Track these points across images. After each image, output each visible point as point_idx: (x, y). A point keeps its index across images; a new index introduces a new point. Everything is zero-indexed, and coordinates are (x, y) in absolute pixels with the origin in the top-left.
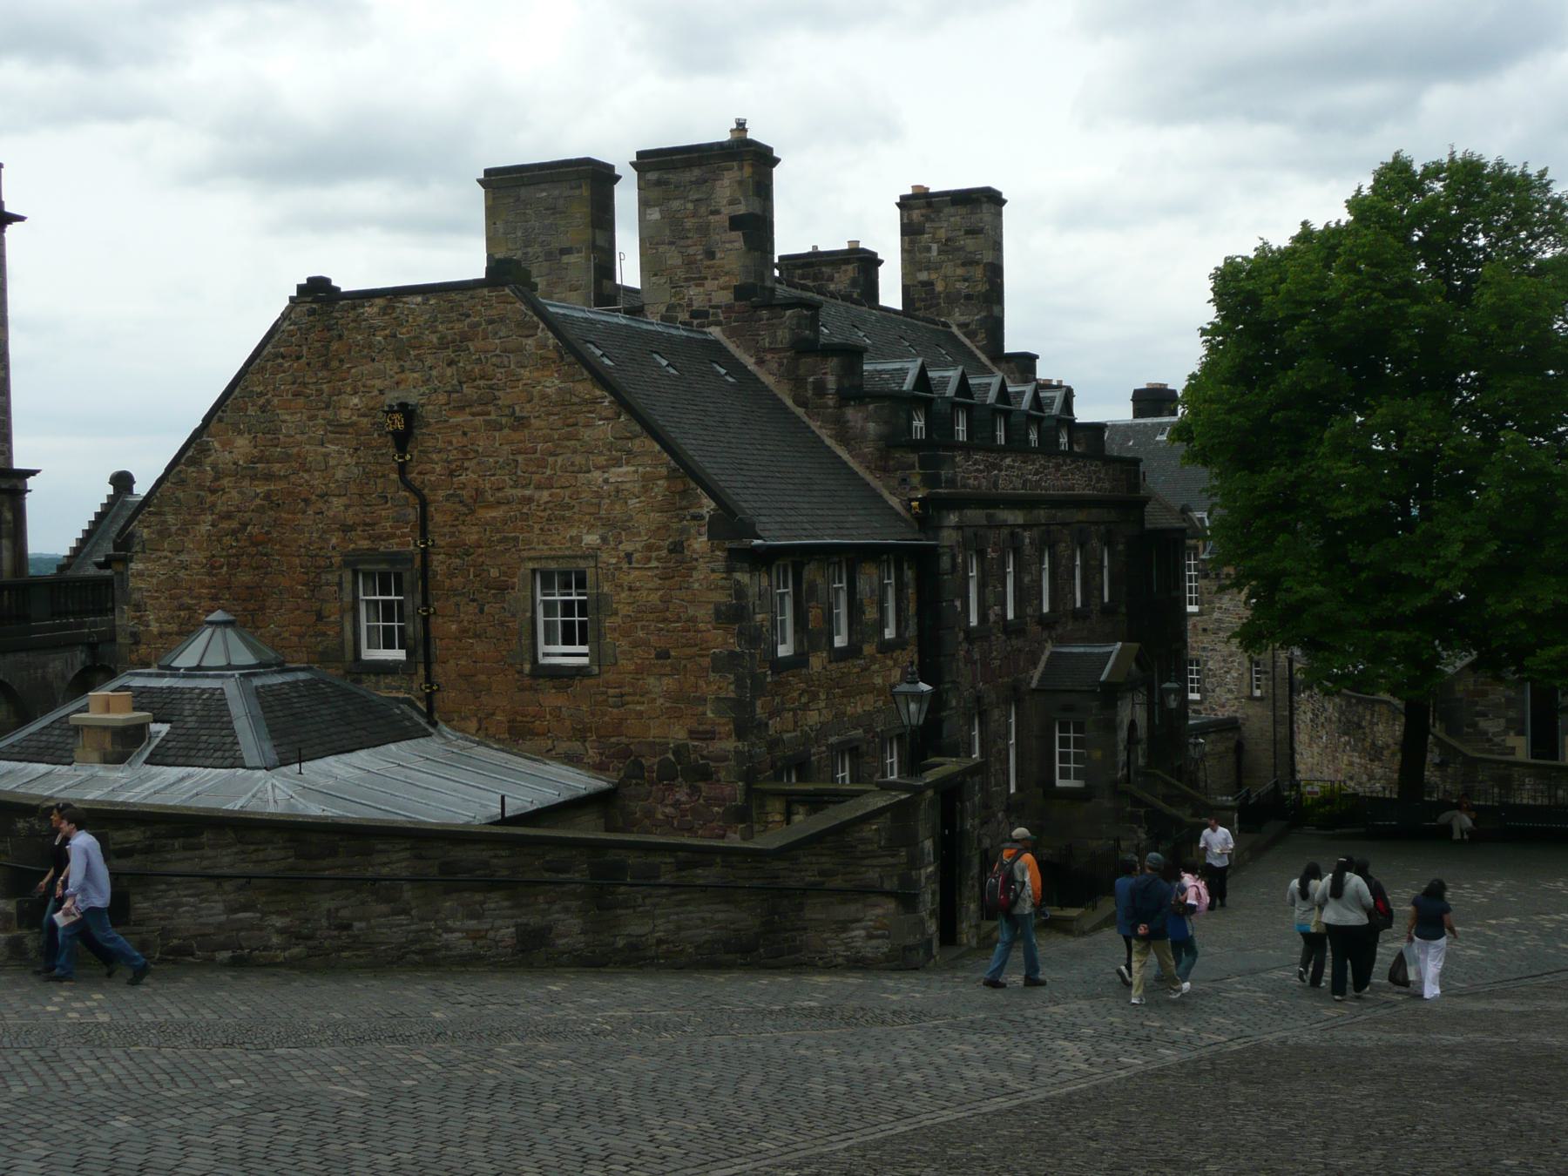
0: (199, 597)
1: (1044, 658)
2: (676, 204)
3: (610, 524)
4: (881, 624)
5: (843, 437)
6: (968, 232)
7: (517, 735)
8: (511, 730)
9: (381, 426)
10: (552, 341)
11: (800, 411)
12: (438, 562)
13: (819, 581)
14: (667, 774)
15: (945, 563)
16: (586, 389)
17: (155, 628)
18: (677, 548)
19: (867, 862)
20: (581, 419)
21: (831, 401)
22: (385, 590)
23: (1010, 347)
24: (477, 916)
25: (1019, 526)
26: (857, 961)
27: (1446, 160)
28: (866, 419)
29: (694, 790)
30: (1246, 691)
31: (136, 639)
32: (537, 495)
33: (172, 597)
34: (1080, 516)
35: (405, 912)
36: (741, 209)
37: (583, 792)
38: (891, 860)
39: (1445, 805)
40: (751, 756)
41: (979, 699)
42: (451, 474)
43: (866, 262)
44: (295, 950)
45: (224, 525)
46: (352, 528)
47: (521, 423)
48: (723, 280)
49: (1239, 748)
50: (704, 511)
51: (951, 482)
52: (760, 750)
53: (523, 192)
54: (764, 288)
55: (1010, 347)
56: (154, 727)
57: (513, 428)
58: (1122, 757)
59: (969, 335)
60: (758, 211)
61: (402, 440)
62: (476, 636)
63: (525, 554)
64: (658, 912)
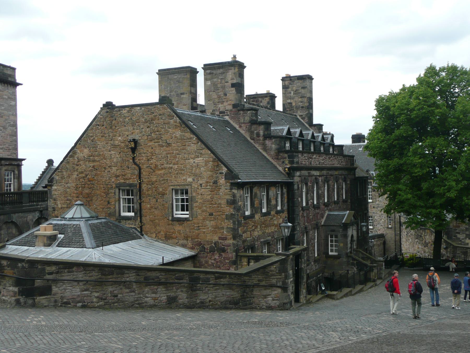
0: (73, 197)
1: (326, 216)
2: (215, 80)
3: (195, 175)
4: (276, 205)
5: (265, 149)
6: (302, 88)
7: (168, 238)
8: (166, 237)
9: (127, 146)
10: (178, 120)
11: (252, 141)
12: (144, 186)
13: (258, 192)
14: (212, 250)
15: (296, 187)
18: (215, 182)
19: (272, 277)
20: (187, 143)
21: (261, 138)
22: (128, 195)
23: (315, 122)
24: (156, 293)
25: (318, 176)
26: (269, 307)
27: (446, 66)
28: (272, 144)
29: (220, 255)
30: (386, 226)
31: (54, 209)
32: (173, 166)
33: (65, 197)
34: (336, 173)
35: (134, 292)
36: (235, 81)
37: (187, 256)
38: (280, 277)
39: (447, 261)
40: (237, 245)
41: (306, 228)
42: (148, 160)
43: (272, 97)
44: (101, 303)
45: (81, 175)
46: (118, 176)
47: (169, 145)
48: (229, 102)
49: (384, 243)
50: (224, 171)
51: (298, 163)
52: (240, 243)
53: (170, 76)
54: (241, 104)
55: (315, 122)
56: (59, 236)
57: (167, 147)
58: (349, 245)
60: (240, 82)
61: (133, 150)
62: (155, 209)
63: (170, 184)
64: (209, 292)
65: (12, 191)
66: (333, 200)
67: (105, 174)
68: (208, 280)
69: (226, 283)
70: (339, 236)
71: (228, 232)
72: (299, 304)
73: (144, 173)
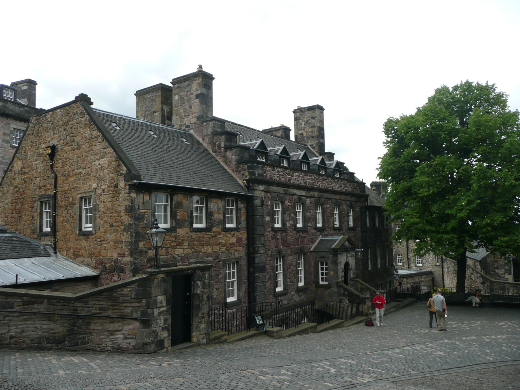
1: (317, 241)
2: (182, 93)
5: (226, 162)
6: (312, 118)
7: (75, 256)
11: (214, 154)
12: (59, 197)
15: (257, 202)
16: (96, 133)
18: (116, 186)
19: (124, 305)
20: (94, 144)
25: (303, 196)
26: (118, 349)
27: (459, 85)
28: (232, 155)
30: (435, 264)
36: (199, 92)
37: (80, 276)
38: (137, 304)
39: (470, 294)
40: (135, 263)
42: (63, 167)
43: (286, 130)
49: (433, 280)
53: (145, 96)
55: (326, 151)
59: (313, 148)
62: (67, 222)
63: (79, 192)
64: (11, 324)
66: (331, 225)
67: (31, 186)
68: (11, 306)
69: (42, 310)
70: (329, 263)
71: (126, 246)
72: (189, 344)
73: (60, 182)
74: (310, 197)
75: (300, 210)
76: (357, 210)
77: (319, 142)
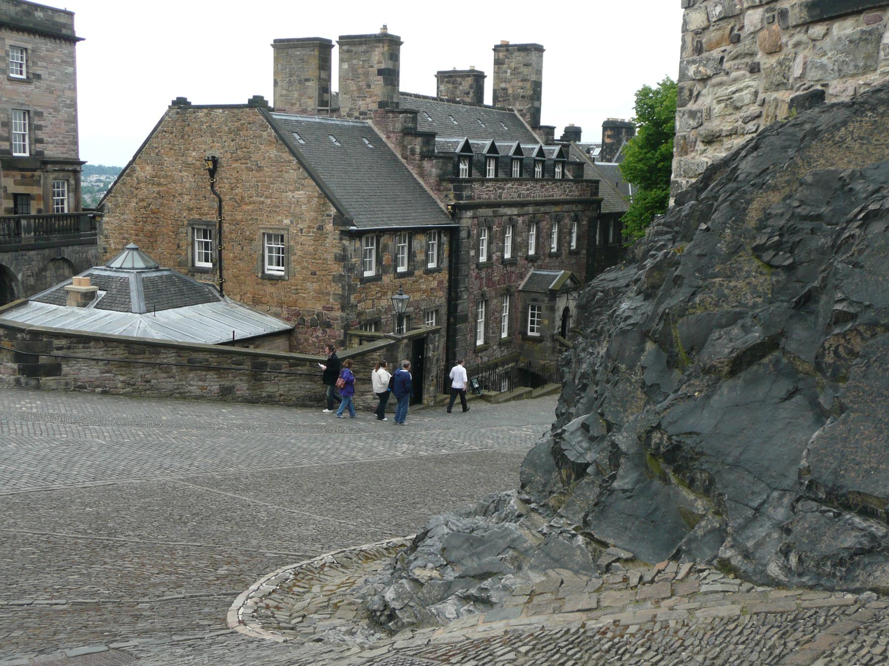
0: (131, 234)
2: (355, 62)
3: (294, 215)
5: (422, 175)
6: (524, 65)
7: (256, 303)
8: (253, 301)
9: (204, 166)
10: (274, 134)
11: (404, 161)
12: (226, 227)
13: (390, 243)
14: (314, 324)
15: (463, 234)
16: (287, 156)
17: (113, 246)
18: (321, 228)
21: (417, 157)
22: (205, 237)
23: (544, 122)
24: (204, 381)
28: (432, 167)
29: (324, 332)
32: (266, 200)
33: (120, 234)
34: (557, 209)
35: (172, 377)
36: (383, 66)
41: (483, 295)
42: (232, 189)
43: (478, 77)
44: (128, 389)
45: (141, 204)
46: (192, 209)
47: (260, 169)
48: (374, 98)
50: (332, 213)
51: (470, 197)
52: (353, 316)
53: (290, 51)
54: (392, 103)
55: (544, 122)
56: (99, 292)
59: (522, 115)
60: (391, 67)
61: (212, 173)
65: (66, 211)
66: (547, 251)
67: (174, 204)
68: (279, 367)
69: (305, 372)
70: (543, 309)
71: (334, 299)
72: (421, 406)
73: (226, 208)
74: (523, 215)
75: (509, 235)
76: (584, 223)
77: (533, 107)
